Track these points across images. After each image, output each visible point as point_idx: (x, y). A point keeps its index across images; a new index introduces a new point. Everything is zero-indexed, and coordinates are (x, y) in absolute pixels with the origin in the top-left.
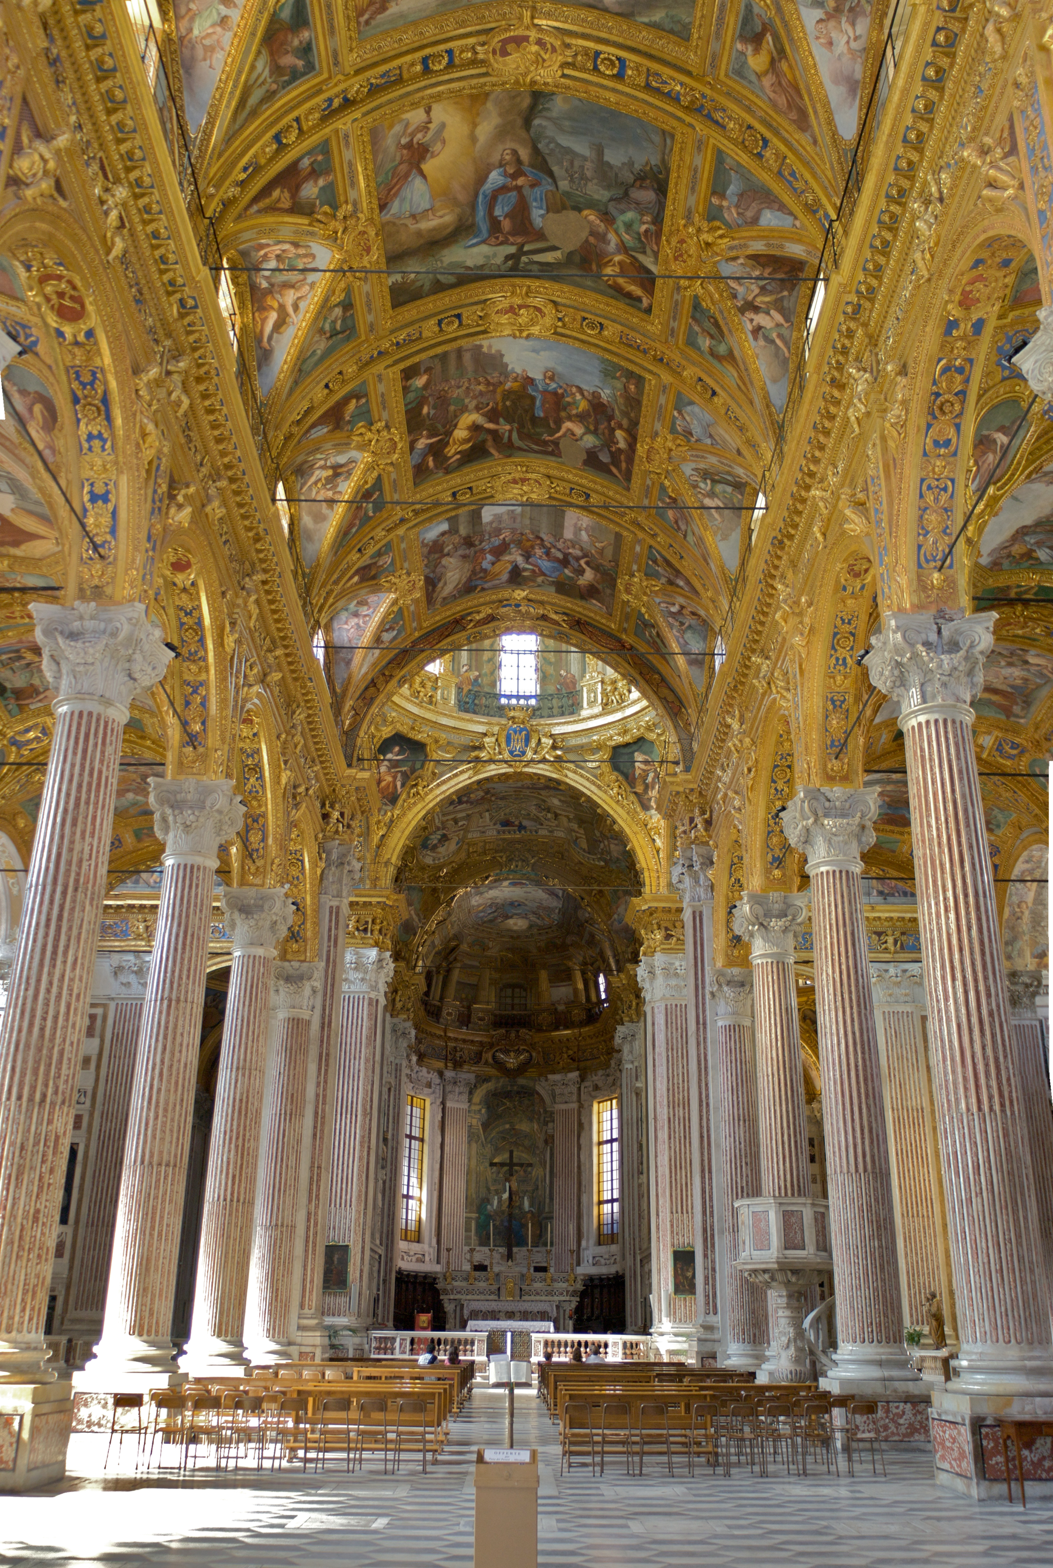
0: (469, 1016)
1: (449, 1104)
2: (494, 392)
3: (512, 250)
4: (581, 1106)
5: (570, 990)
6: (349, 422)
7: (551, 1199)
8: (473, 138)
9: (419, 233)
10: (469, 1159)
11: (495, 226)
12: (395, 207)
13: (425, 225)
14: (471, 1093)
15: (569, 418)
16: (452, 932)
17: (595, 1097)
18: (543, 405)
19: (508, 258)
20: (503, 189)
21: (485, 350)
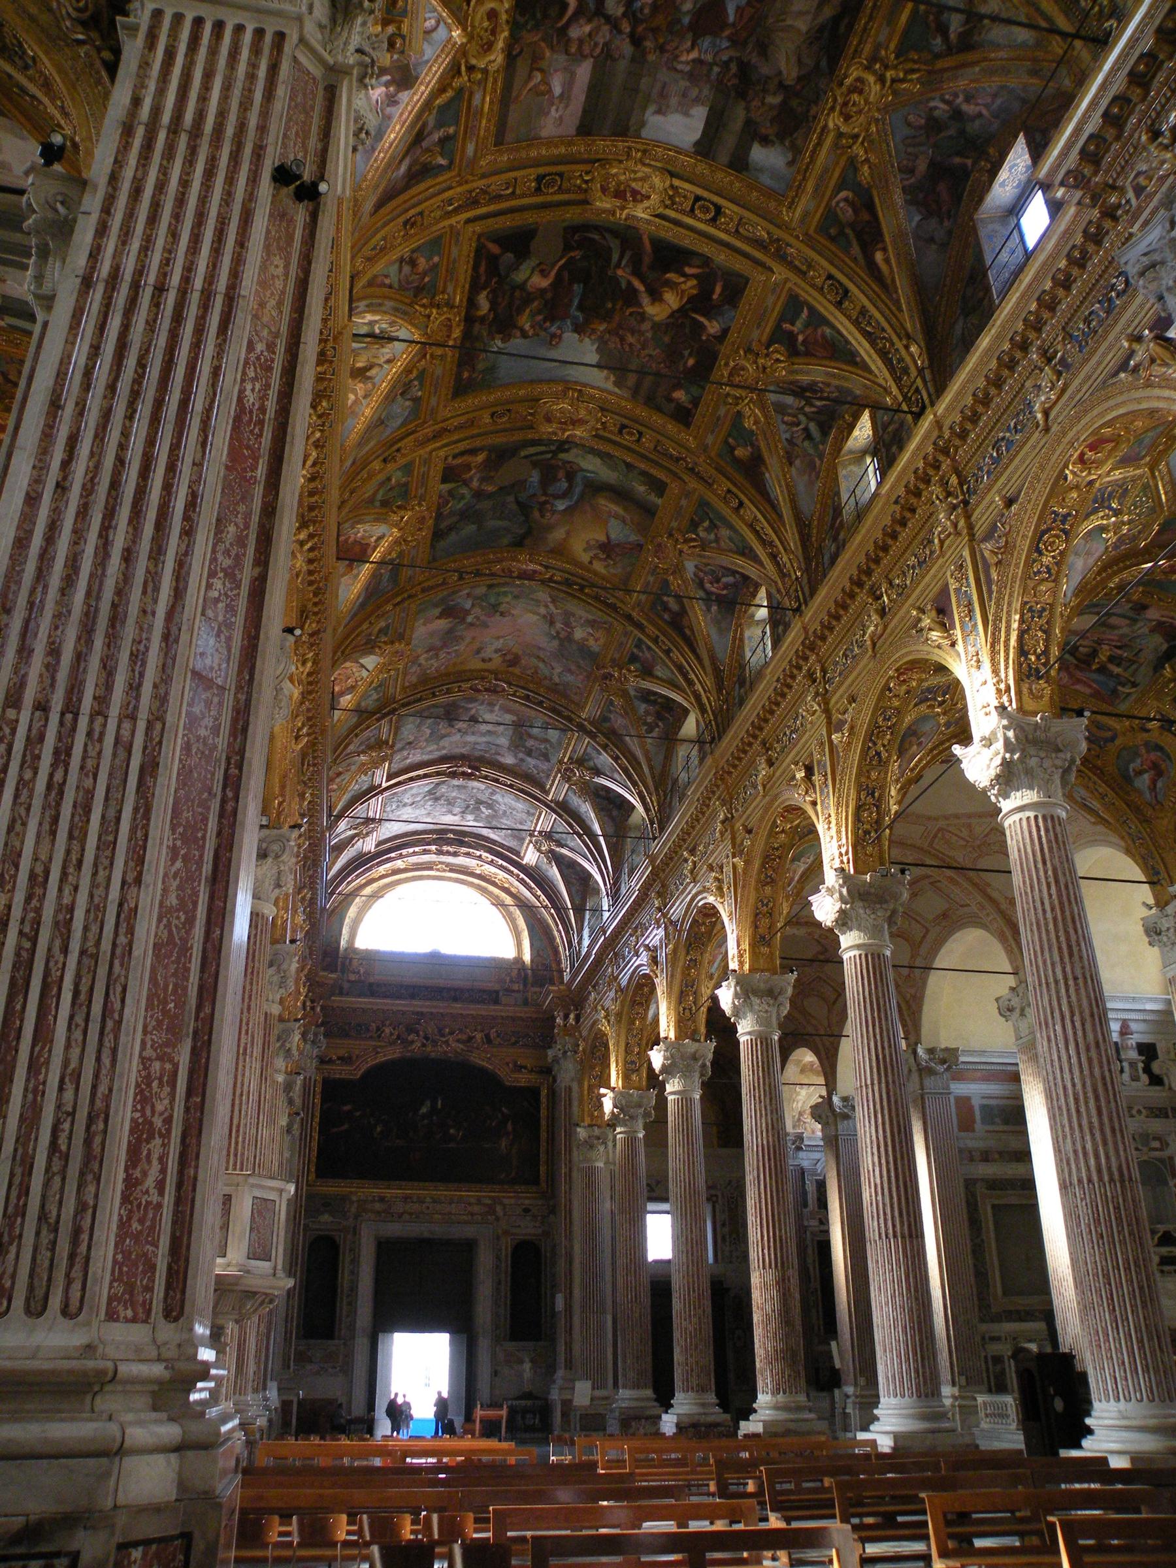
2: (620, 326)
3: (562, 456)
6: (752, 445)
8: (568, 533)
9: (625, 509)
11: (570, 476)
12: (633, 538)
13: (621, 512)
15: (543, 291)
18: (571, 301)
19: (567, 451)
20: (557, 497)
21: (612, 378)
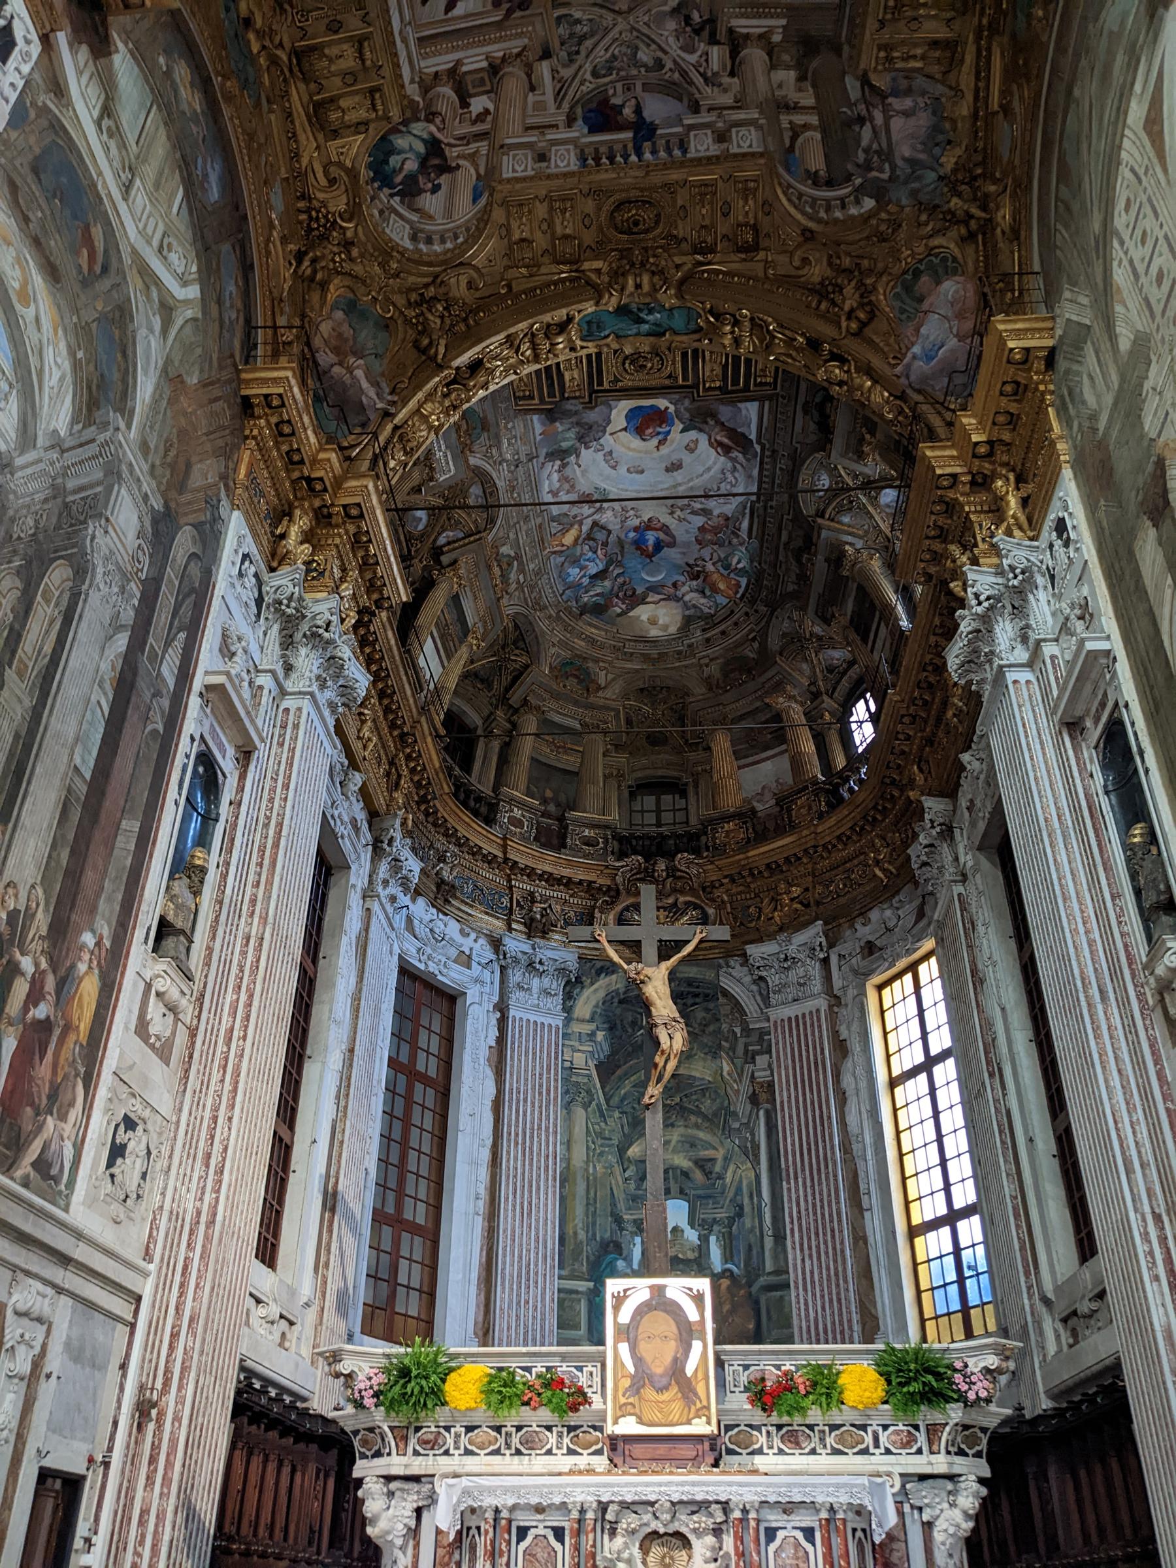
0: (563, 837)
1: (512, 1013)
4: (836, 1001)
5: (784, 762)
7: (780, 1238)
10: (568, 1144)
14: (569, 996)
16: (510, 607)
17: (868, 974)
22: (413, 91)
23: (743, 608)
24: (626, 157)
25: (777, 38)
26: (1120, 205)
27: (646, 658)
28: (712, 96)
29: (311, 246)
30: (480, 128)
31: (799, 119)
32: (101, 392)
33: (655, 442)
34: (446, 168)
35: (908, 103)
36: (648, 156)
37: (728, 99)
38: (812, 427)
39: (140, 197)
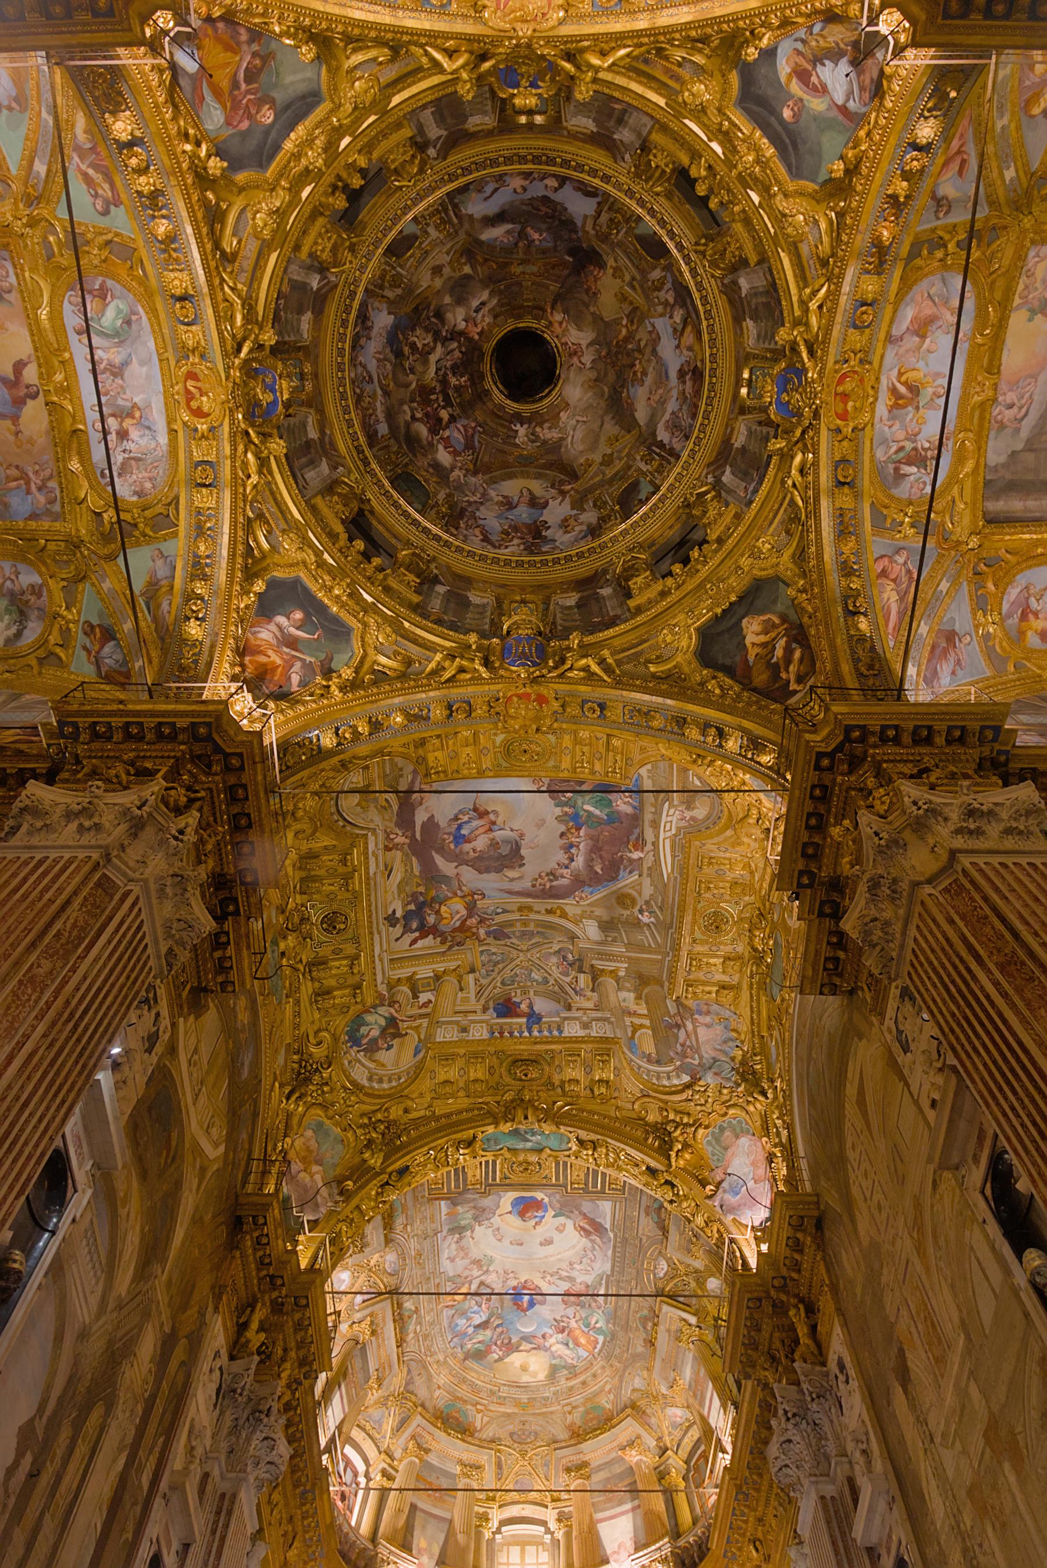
22: (383, 989)
23: (599, 1363)
24: (521, 1033)
25: (622, 974)
26: (849, 1145)
27: (517, 1403)
28: (579, 1001)
29: (299, 1086)
30: (423, 1011)
31: (637, 1021)
32: (153, 1250)
33: (533, 1222)
34: (398, 1035)
35: (708, 1019)
36: (536, 1033)
37: (590, 1005)
38: (652, 1224)
39: (202, 1100)
